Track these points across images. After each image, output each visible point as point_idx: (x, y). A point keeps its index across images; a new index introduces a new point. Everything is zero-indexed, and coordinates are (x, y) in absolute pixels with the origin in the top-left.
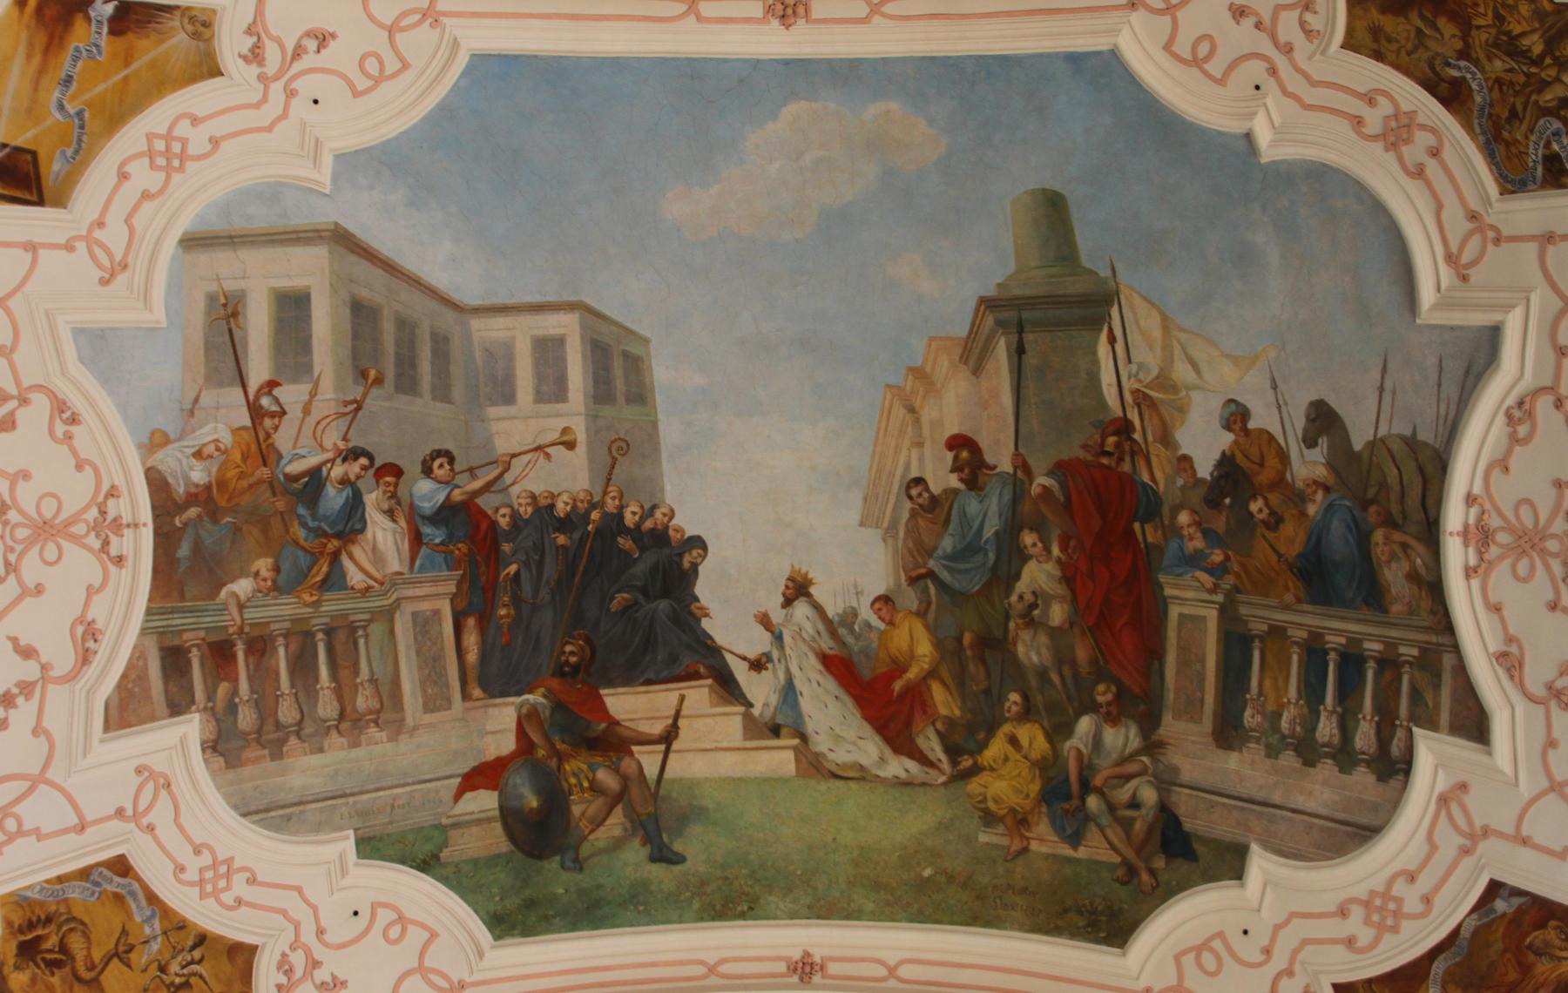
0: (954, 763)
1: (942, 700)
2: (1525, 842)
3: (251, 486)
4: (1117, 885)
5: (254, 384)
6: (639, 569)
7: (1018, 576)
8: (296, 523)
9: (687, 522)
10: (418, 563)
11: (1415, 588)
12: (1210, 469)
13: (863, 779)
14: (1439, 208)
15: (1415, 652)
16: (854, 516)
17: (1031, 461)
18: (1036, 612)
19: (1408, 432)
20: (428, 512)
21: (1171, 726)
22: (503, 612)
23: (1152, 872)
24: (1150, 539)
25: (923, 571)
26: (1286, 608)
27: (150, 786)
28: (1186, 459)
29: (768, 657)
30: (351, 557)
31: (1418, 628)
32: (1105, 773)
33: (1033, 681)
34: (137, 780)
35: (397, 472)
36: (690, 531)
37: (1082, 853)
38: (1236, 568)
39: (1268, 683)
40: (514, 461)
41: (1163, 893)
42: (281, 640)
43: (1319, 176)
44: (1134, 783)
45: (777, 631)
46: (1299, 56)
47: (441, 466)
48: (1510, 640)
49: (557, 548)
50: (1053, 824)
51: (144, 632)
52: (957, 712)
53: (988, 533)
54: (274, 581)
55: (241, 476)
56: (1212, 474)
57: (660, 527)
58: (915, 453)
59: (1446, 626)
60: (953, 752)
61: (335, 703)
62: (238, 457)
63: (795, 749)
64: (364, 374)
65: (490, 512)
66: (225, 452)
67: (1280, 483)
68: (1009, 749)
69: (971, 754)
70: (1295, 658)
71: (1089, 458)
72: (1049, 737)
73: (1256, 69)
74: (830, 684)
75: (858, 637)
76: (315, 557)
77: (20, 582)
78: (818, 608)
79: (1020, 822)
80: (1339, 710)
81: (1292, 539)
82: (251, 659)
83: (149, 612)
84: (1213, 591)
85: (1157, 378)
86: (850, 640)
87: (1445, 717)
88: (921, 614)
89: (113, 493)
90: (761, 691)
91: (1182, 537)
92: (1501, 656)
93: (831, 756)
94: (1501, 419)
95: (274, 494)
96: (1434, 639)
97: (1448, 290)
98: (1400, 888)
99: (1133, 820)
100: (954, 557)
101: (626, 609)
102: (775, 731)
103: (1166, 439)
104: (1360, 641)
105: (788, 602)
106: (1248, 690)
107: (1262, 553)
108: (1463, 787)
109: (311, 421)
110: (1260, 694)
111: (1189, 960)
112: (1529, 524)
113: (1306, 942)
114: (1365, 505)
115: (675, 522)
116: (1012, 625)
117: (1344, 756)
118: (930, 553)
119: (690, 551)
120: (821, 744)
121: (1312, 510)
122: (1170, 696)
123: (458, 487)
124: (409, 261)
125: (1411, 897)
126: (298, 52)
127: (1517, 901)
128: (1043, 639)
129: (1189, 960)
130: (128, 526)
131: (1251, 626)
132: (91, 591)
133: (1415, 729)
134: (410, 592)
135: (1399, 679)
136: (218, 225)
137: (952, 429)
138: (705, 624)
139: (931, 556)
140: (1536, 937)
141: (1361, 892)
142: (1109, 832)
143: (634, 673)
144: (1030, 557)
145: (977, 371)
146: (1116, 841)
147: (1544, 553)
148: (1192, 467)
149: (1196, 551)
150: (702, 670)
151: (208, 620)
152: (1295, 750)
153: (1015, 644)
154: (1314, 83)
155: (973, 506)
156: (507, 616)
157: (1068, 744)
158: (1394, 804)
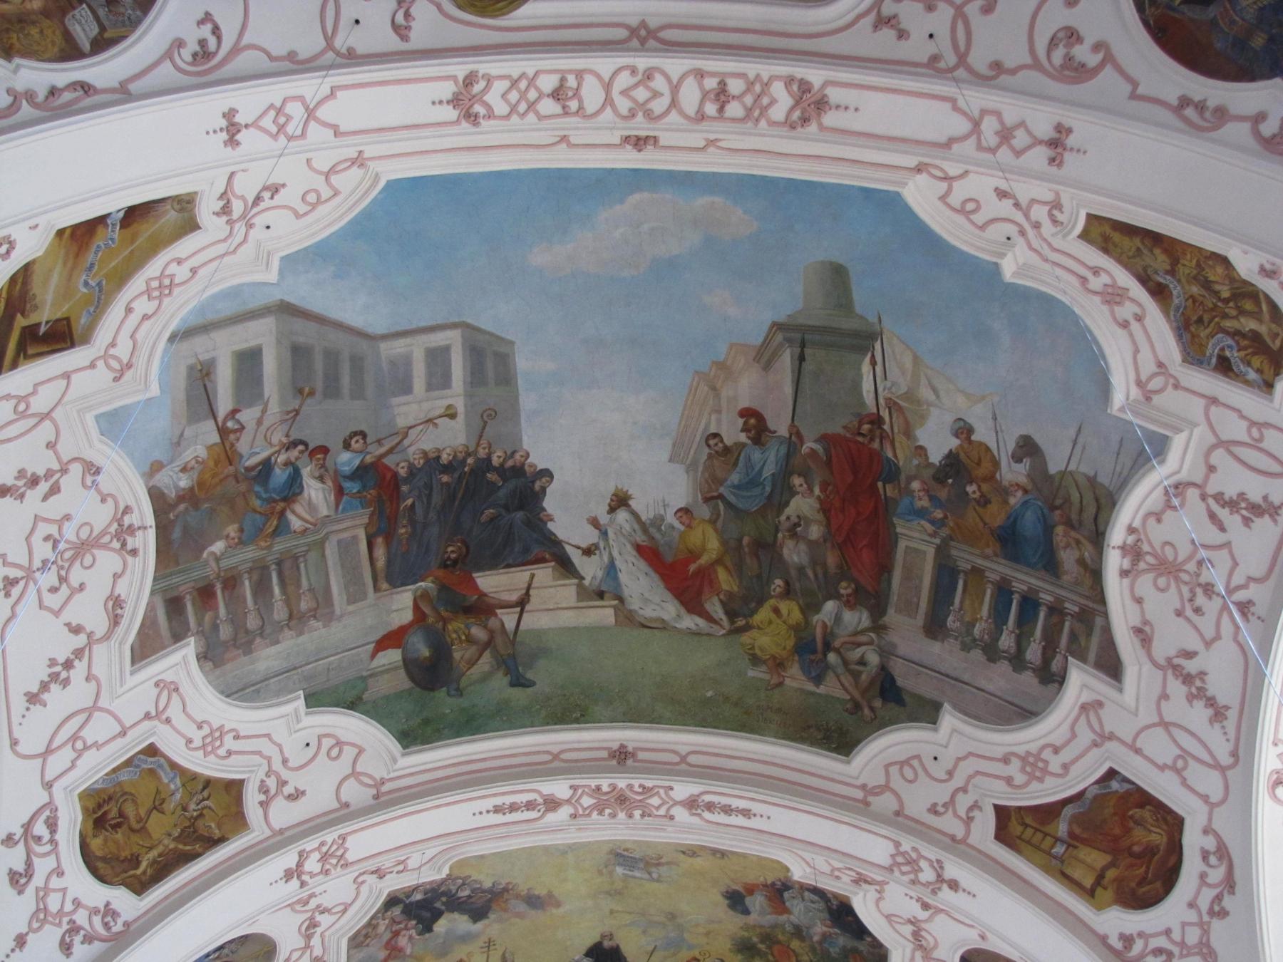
0: (732, 622)
1: (725, 580)
2: (1138, 751)
3: (221, 481)
4: (846, 714)
5: (222, 411)
6: (501, 493)
7: (787, 504)
8: (254, 498)
9: (538, 460)
10: (341, 507)
11: (1082, 570)
12: (940, 459)
13: (665, 628)
14: (1136, 351)
15: (1076, 609)
16: (666, 456)
17: (804, 432)
18: (799, 529)
19: (1092, 474)
20: (348, 473)
21: (892, 617)
22: (402, 531)
23: (872, 709)
24: (889, 494)
25: (715, 494)
26: (986, 557)
27: (165, 693)
28: (921, 448)
29: (596, 546)
30: (294, 512)
31: (1080, 595)
32: (842, 640)
33: (793, 573)
34: (156, 691)
35: (324, 450)
36: (540, 466)
37: (822, 690)
38: (951, 524)
39: (967, 602)
40: (411, 431)
41: (879, 724)
42: (246, 576)
44: (863, 649)
45: (603, 530)
47: (357, 442)
48: (1146, 622)
49: (442, 484)
50: (802, 668)
51: (153, 593)
52: (736, 589)
53: (767, 473)
54: (240, 538)
55: (213, 477)
56: (940, 462)
57: (518, 464)
58: (714, 417)
59: (1102, 600)
60: (732, 614)
61: (286, 609)
62: (211, 464)
63: (614, 607)
65: (393, 467)
66: (203, 462)
67: (990, 478)
68: (773, 616)
69: (745, 617)
70: (989, 592)
71: (848, 435)
72: (802, 611)
74: (643, 565)
75: (663, 535)
76: (267, 516)
77: (69, 586)
78: (635, 515)
79: (778, 665)
80: (1017, 631)
81: (996, 516)
82: (227, 593)
83: (155, 579)
84: (934, 535)
85: (906, 393)
86: (658, 536)
87: (1092, 656)
88: (713, 522)
89: (127, 510)
90: (591, 569)
91: (913, 497)
92: (1138, 631)
93: (641, 612)
95: (238, 482)
96: (1091, 605)
97: (1133, 401)
98: (1047, 754)
99: (860, 673)
100: (738, 487)
101: (493, 520)
102: (601, 595)
103: (908, 433)
104: (1037, 592)
105: (612, 510)
106: (952, 604)
107: (971, 518)
108: (1100, 704)
109: (263, 428)
110: (961, 609)
111: (894, 770)
112: (1171, 558)
113: (978, 773)
114: (1053, 508)
115: (529, 461)
116: (780, 535)
117: (1018, 661)
118: (721, 482)
119: (540, 479)
120: (634, 604)
121: (1012, 501)
122: (894, 598)
123: (368, 453)
125: (1055, 764)
127: (1127, 786)
128: (803, 547)
129: (894, 770)
130: (139, 528)
131: (959, 563)
132: (116, 576)
133: (1070, 658)
134: (335, 528)
135: (1062, 623)
137: (744, 403)
138: (550, 525)
139: (721, 485)
140: (1136, 812)
141: (1021, 750)
142: (843, 678)
143: (496, 561)
144: (798, 493)
145: (767, 367)
146: (847, 684)
147: (1177, 579)
148: (926, 455)
149: (923, 507)
150: (547, 556)
151: (195, 574)
152: (983, 650)
153: (782, 548)
155: (756, 455)
156: (406, 533)
157: (816, 617)
158: (1048, 703)
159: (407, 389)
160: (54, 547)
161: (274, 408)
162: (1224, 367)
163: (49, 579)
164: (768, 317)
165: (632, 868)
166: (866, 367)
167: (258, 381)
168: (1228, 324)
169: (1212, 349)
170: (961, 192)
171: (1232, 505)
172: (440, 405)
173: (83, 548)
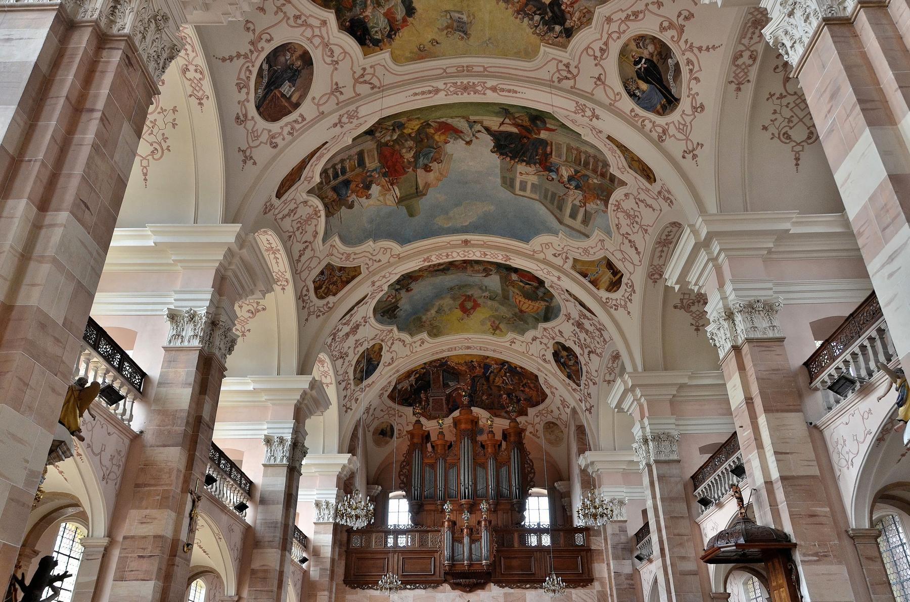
9: (495, 156)
29: (476, 132)
43: (360, 241)
53: (422, 158)
64: (563, 199)
81: (353, 186)
86: (456, 136)
88: (438, 142)
94: (318, 232)
103: (383, 186)
105: (471, 141)
107: (359, 179)
126: (559, 255)
136: (583, 237)
137: (431, 174)
155: (426, 162)
159: (533, 184)
160: (633, 224)
161: (570, 200)
162: (322, 273)
163: (637, 219)
164: (427, 197)
165: (459, 21)
166: (398, 195)
167: (572, 209)
168: (327, 281)
169: (326, 273)
170: (388, 255)
171: (304, 250)
172: (523, 176)
173: (629, 216)
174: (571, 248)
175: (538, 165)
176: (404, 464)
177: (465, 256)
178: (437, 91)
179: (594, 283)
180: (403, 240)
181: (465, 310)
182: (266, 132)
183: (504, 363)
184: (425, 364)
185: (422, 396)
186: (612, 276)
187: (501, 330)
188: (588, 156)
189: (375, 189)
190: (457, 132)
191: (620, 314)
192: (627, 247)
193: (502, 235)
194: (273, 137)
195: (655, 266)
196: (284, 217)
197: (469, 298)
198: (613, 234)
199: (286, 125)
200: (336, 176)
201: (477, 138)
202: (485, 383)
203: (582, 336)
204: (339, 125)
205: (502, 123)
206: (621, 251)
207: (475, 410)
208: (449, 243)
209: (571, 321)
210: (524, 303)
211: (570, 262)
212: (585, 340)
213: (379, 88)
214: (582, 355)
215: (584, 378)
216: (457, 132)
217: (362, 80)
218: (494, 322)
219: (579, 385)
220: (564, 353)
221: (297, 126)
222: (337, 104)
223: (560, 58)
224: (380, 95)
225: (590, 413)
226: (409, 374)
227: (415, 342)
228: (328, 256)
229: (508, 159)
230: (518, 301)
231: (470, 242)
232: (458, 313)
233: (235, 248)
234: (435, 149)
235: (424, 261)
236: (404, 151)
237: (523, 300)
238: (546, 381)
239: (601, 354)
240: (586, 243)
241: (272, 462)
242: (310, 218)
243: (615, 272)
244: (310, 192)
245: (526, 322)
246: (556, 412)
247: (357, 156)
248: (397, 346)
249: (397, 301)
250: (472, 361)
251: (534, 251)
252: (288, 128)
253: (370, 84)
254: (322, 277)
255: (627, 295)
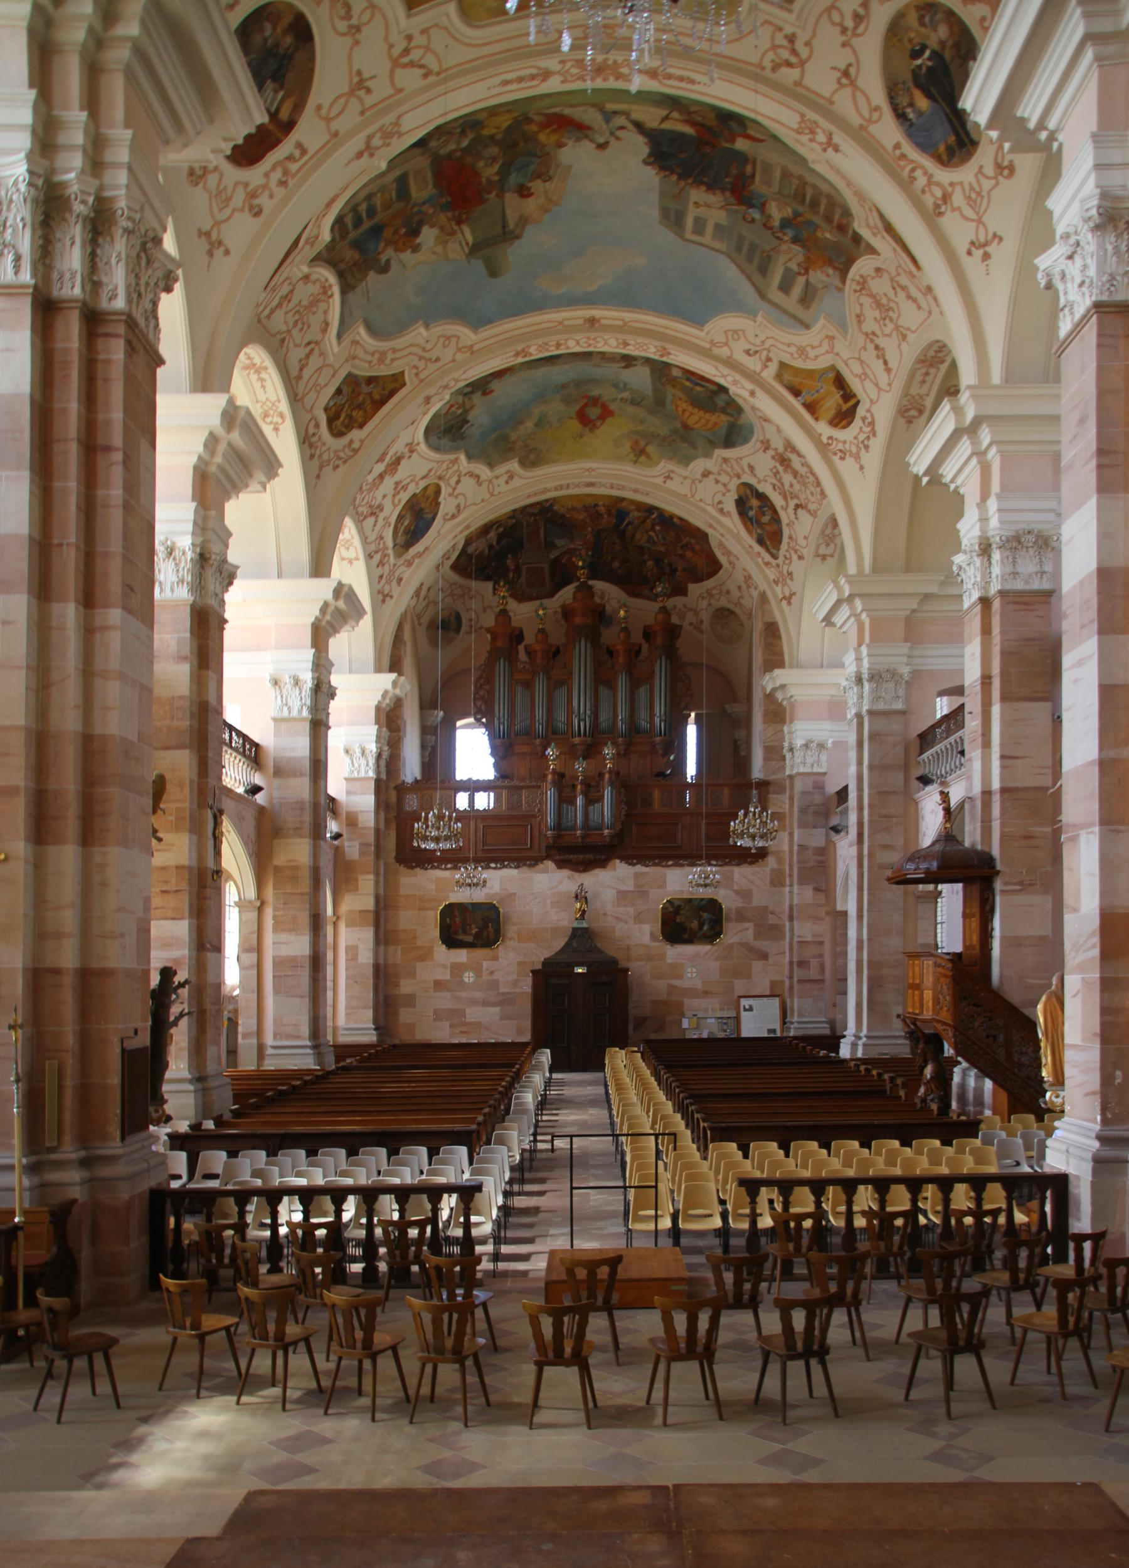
46: (416, 358)
64: (769, 257)
73: (428, 347)
81: (388, 233)
89: (855, 291)
103: (442, 228)
124: (743, 278)
126: (756, 352)
137: (531, 200)
154: (410, 354)
161: (782, 259)
162: (339, 391)
169: (345, 389)
170: (451, 349)
171: (308, 356)
173: (879, 305)
174: (777, 344)
175: (728, 194)
176: (482, 681)
177: (589, 345)
178: (546, 75)
179: (811, 408)
180: (478, 322)
181: (583, 418)
182: (240, 189)
183: (651, 509)
184: (514, 511)
185: (510, 563)
186: (841, 402)
187: (648, 456)
188: (818, 192)
189: (428, 235)
190: (581, 129)
191: (848, 468)
192: (870, 356)
193: (658, 310)
194: (253, 195)
195: (913, 397)
196: (273, 311)
197: (595, 401)
198: (850, 331)
199: (274, 168)
200: (358, 222)
201: (618, 139)
202: (617, 541)
203: (787, 478)
204: (366, 154)
205: (666, 118)
206: (862, 362)
207: (598, 585)
208: (560, 323)
209: (771, 453)
210: (692, 414)
211: (773, 367)
212: (791, 486)
213: (438, 74)
214: (785, 509)
215: (784, 546)
216: (581, 129)
217: (405, 60)
218: (637, 442)
219: (775, 557)
220: (755, 502)
221: (293, 167)
222: (362, 113)
223: (779, 23)
224: (441, 89)
225: (789, 603)
226: (486, 529)
227: (497, 478)
228: (347, 361)
229: (674, 178)
230: (680, 409)
231: (598, 321)
232: (575, 425)
233: (220, 432)
234: (539, 157)
235: (517, 355)
236: (481, 164)
237: (690, 408)
238: (721, 544)
239: (815, 512)
240: (804, 338)
241: (285, 713)
242: (314, 303)
243: (848, 395)
244: (316, 259)
245: (693, 445)
246: (735, 593)
247: (394, 185)
248: (467, 484)
249: (466, 412)
250: (596, 505)
251: (711, 342)
252: (277, 175)
253: (422, 66)
254: (341, 400)
255: (862, 437)
